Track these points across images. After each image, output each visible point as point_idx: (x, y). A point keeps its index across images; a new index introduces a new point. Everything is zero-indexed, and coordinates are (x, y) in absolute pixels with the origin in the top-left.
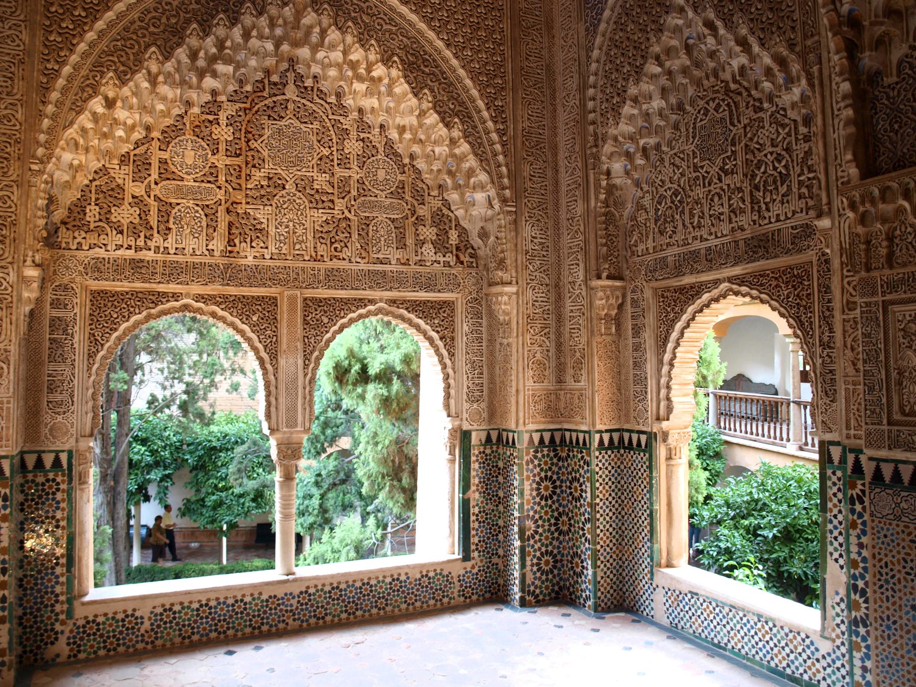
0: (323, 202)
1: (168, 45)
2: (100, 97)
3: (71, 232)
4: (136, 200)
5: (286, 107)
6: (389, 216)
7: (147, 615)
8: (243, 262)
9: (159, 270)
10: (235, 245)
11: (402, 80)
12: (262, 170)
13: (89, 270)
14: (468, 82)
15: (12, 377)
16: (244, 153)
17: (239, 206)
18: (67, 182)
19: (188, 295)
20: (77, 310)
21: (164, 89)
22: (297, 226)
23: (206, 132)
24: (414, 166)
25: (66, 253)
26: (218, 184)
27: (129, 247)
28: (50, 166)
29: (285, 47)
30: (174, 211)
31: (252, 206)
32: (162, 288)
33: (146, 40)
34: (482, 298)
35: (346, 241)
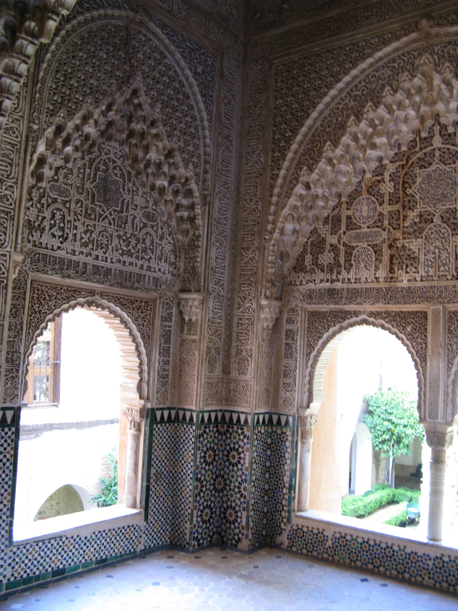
2: (300, 185)
5: (434, 156)
7: (330, 536)
8: (399, 285)
9: (345, 295)
15: (253, 366)
17: (398, 242)
18: (295, 242)
19: (364, 312)
20: (299, 325)
21: (343, 167)
22: (442, 252)
23: (376, 190)
25: (295, 288)
26: (383, 227)
27: (327, 281)
30: (354, 252)
31: (407, 240)
32: (347, 308)
33: (325, 138)
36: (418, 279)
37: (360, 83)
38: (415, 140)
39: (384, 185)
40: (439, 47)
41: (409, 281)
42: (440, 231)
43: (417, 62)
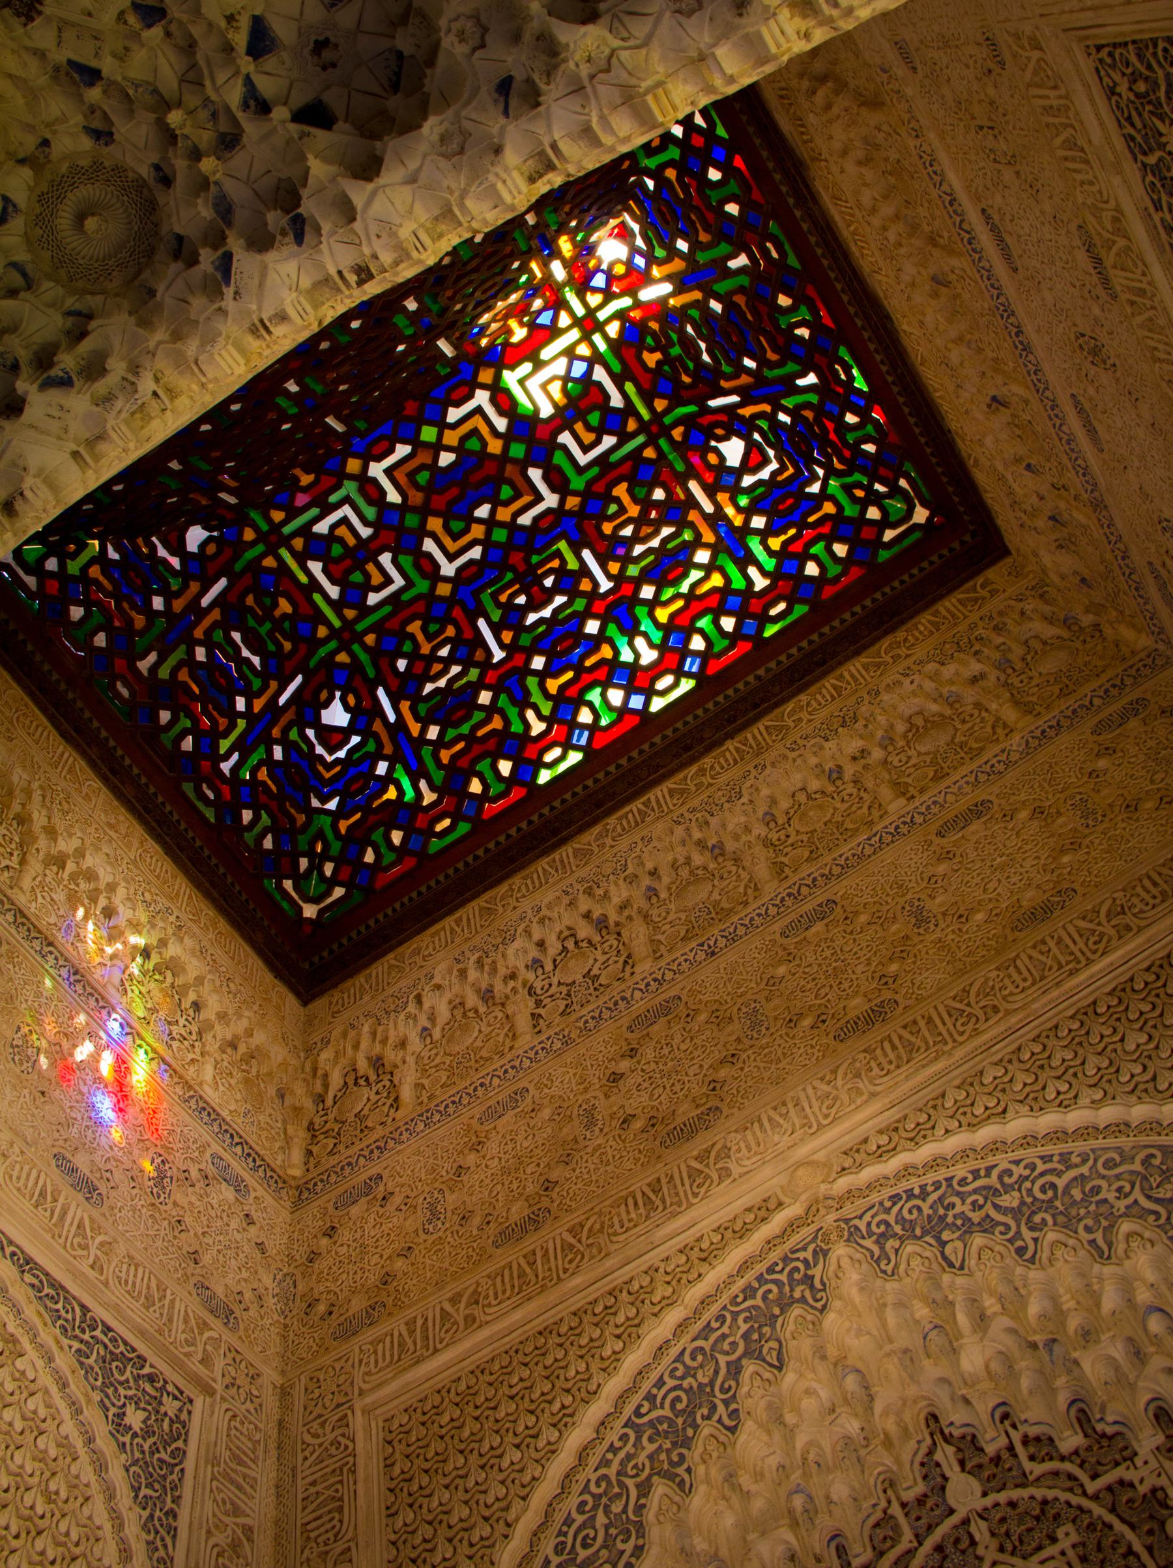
37: (660, 1383)
38: (887, 1517)
40: (867, 1217)
43: (817, 1272)
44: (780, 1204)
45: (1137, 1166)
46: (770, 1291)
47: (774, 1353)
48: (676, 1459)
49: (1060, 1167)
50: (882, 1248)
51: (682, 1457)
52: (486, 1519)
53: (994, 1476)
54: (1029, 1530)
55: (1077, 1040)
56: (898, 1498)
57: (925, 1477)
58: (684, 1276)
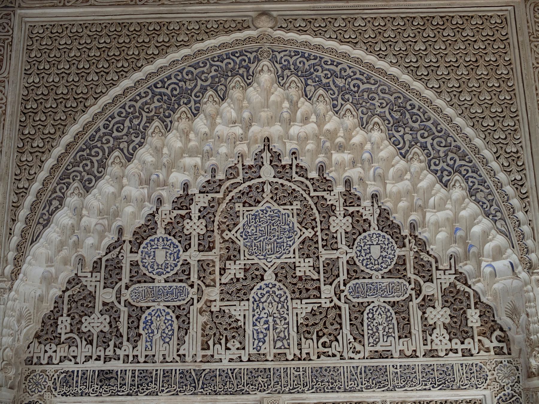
0: (307, 290)
1: (131, 147)
2: (65, 208)
3: (42, 346)
4: (106, 308)
5: (263, 191)
6: (387, 300)
9: (128, 379)
10: (208, 348)
11: (386, 142)
12: (237, 262)
13: (58, 384)
14: (469, 131)
16: (217, 245)
22: (278, 321)
23: (179, 227)
24: (416, 237)
25: (39, 368)
26: (190, 282)
27: (98, 359)
28: (17, 283)
29: (255, 129)
30: (143, 317)
34: (520, 395)
35: (336, 333)
36: (245, 358)
37: (169, 78)
39: (191, 224)
40: (282, 54)
41: (231, 360)
42: (274, 292)
43: (253, 66)
44: (249, 27)
45: (392, 98)
46: (230, 63)
47: (222, 92)
48: (167, 114)
49: (365, 80)
50: (283, 72)
51: (170, 114)
52: (75, 99)
53: (281, 172)
54: (284, 196)
55: (399, 30)
56: (242, 161)
57: (255, 159)
58: (196, 35)
